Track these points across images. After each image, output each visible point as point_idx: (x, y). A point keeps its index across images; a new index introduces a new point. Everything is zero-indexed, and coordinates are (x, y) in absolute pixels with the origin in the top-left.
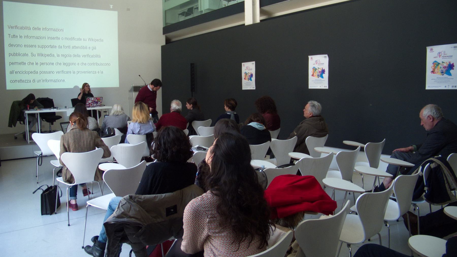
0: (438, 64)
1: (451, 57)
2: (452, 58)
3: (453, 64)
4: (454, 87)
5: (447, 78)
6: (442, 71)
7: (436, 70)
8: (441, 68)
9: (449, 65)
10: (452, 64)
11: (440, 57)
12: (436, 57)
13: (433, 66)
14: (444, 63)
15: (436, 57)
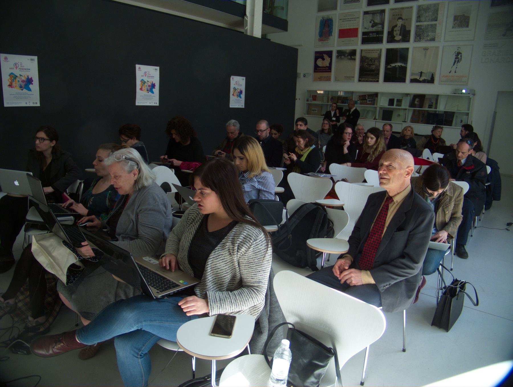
0: (15, 77)
1: (29, 70)
2: (30, 71)
3: (31, 78)
4: (35, 103)
5: (27, 93)
6: (20, 86)
7: (14, 84)
8: (19, 81)
9: (27, 79)
10: (30, 78)
11: (16, 69)
12: (12, 69)
13: (10, 79)
14: (22, 76)
15: (12, 69)
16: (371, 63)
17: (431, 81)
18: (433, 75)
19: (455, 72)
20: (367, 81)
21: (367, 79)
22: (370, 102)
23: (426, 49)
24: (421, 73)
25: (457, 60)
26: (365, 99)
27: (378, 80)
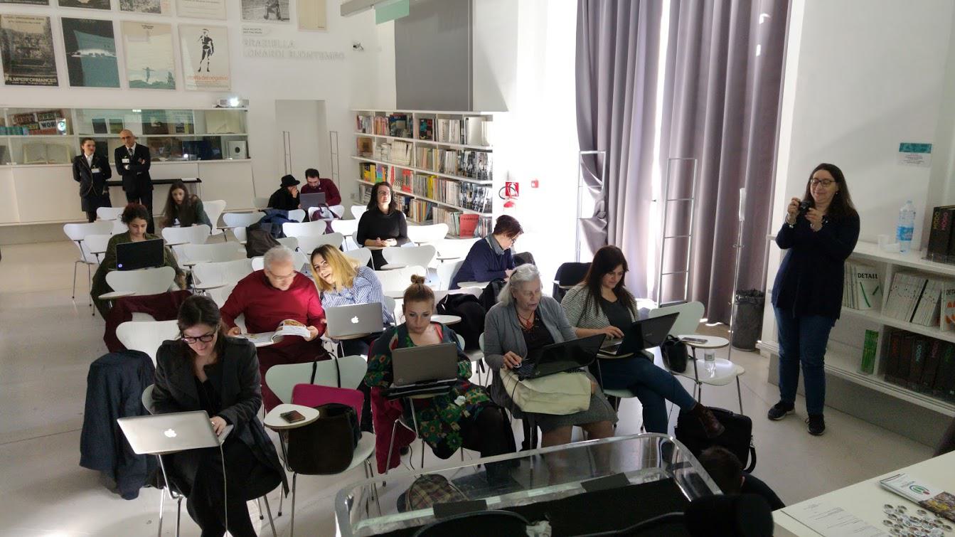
16: (30, 46)
17: (171, 85)
18: (170, 74)
19: (208, 71)
20: (27, 84)
21: (27, 80)
22: (47, 128)
23: (148, 27)
24: (148, 69)
25: (207, 50)
26: (33, 122)
27: (56, 81)
